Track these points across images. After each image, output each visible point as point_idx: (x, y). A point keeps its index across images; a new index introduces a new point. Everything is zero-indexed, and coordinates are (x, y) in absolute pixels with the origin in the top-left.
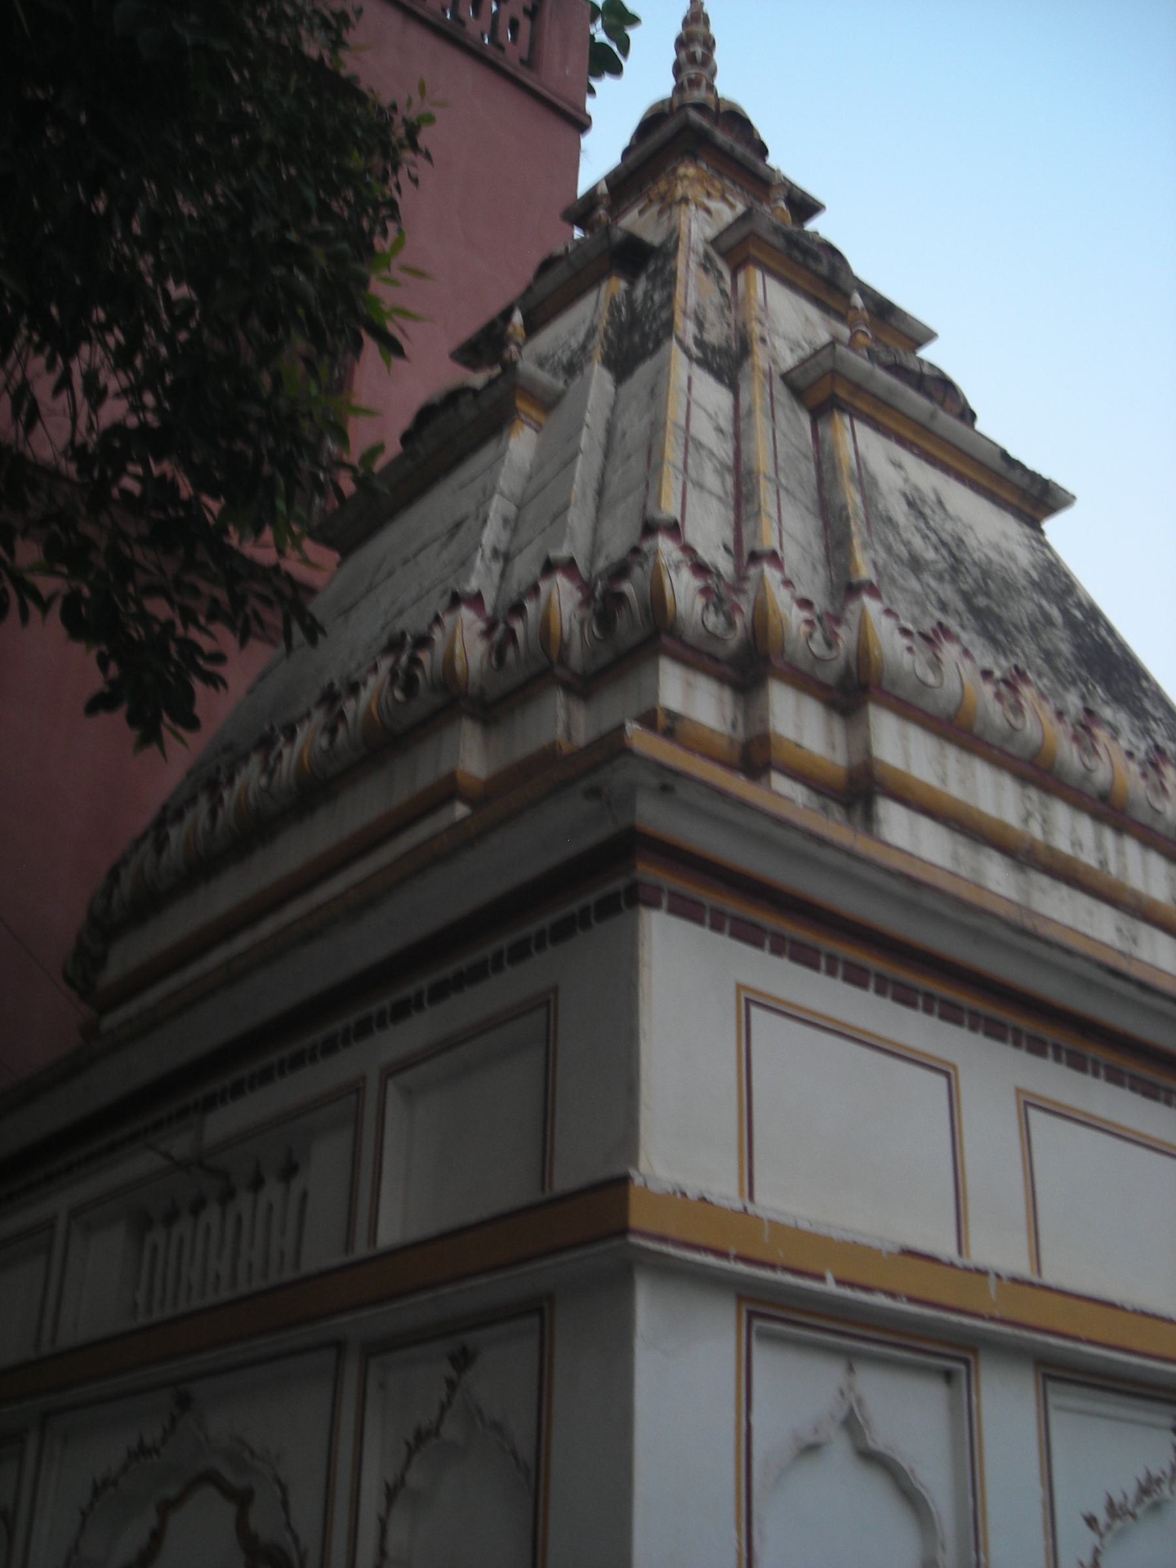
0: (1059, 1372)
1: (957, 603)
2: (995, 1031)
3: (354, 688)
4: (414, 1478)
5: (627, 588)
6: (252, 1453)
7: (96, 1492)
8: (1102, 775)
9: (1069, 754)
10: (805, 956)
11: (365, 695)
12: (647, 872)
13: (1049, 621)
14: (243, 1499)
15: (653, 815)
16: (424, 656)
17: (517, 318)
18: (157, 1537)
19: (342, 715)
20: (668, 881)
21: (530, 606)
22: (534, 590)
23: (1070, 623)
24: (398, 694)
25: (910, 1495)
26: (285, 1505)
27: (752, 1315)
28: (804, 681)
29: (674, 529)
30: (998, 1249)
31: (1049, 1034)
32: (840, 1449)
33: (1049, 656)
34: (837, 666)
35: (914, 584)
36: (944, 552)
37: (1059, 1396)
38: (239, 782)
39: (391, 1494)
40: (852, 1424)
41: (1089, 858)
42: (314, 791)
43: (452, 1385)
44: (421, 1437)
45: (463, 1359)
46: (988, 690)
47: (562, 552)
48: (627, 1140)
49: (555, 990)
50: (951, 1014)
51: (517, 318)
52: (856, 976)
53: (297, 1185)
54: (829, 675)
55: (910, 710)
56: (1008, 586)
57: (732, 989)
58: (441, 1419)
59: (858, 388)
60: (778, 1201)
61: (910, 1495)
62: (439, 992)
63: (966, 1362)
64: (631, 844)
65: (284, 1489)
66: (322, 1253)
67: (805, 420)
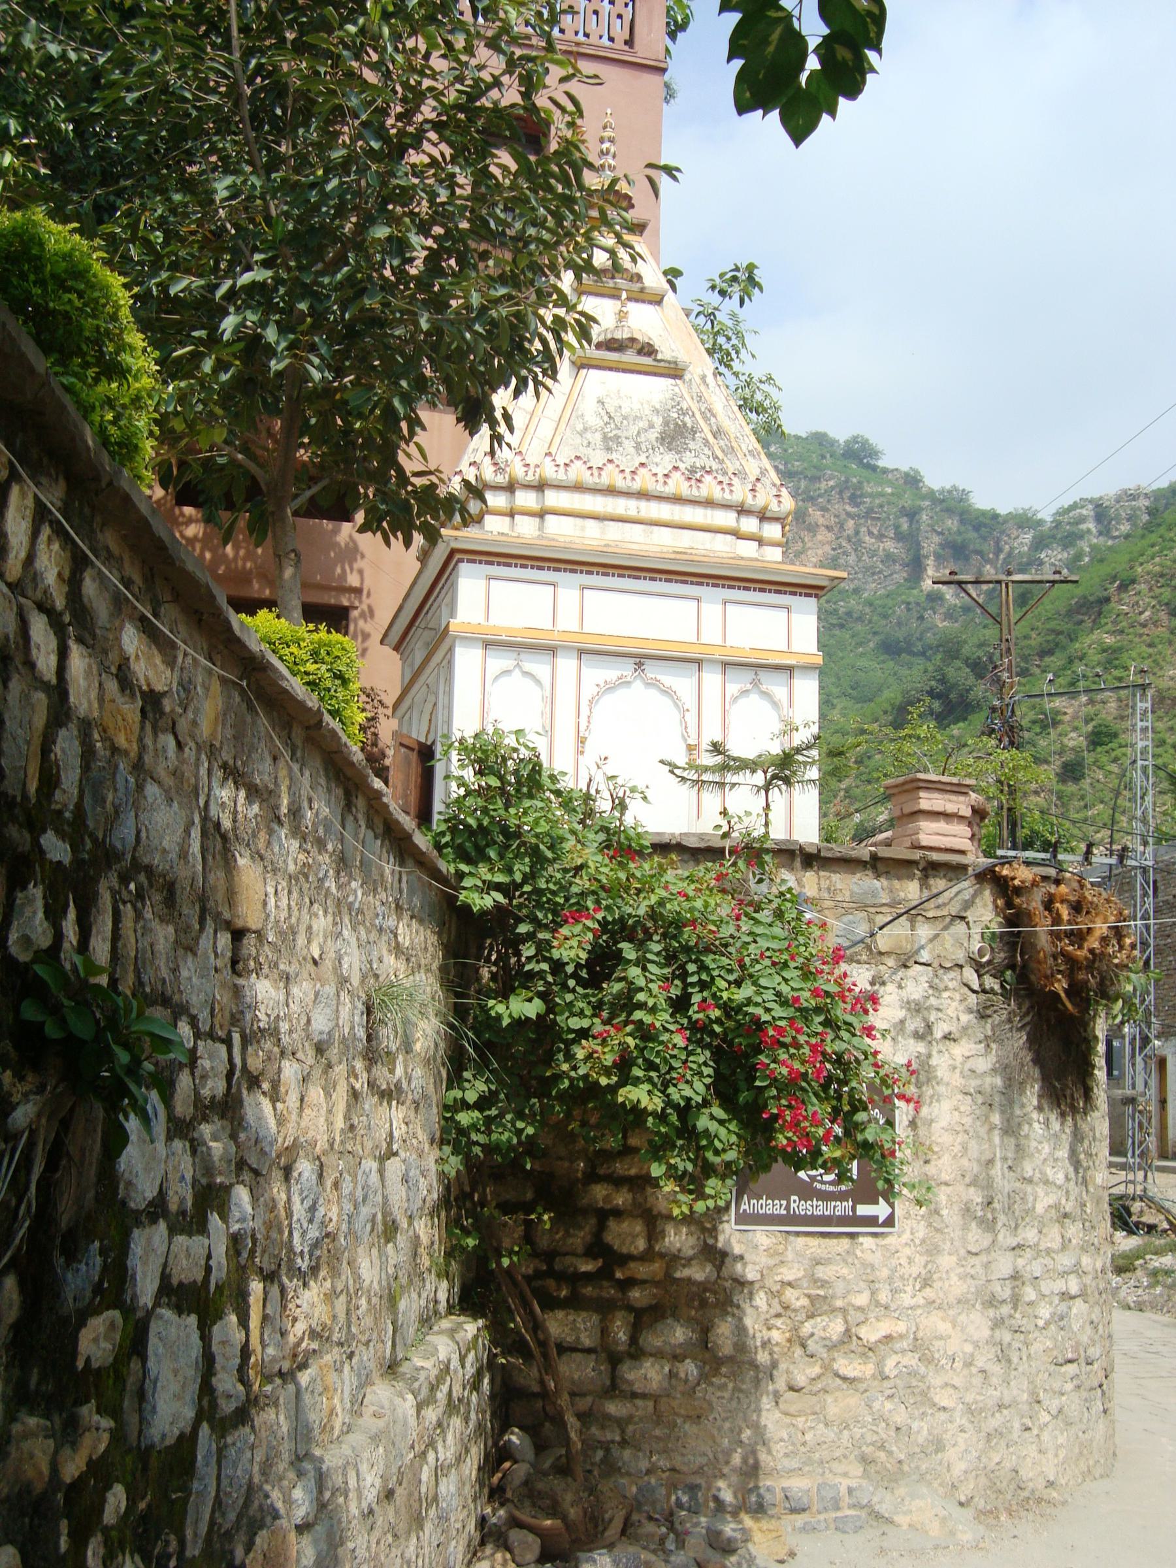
0: (582, 652)
2: (572, 571)
8: (636, 486)
9: (620, 483)
10: (509, 565)
13: (651, 426)
20: (466, 557)
23: (666, 423)
25: (538, 682)
28: (528, 487)
31: (595, 569)
32: (517, 672)
33: (638, 447)
35: (578, 440)
36: (606, 419)
41: (632, 513)
50: (555, 570)
52: (524, 566)
55: (559, 487)
56: (637, 418)
60: (491, 623)
61: (538, 682)
64: (453, 552)
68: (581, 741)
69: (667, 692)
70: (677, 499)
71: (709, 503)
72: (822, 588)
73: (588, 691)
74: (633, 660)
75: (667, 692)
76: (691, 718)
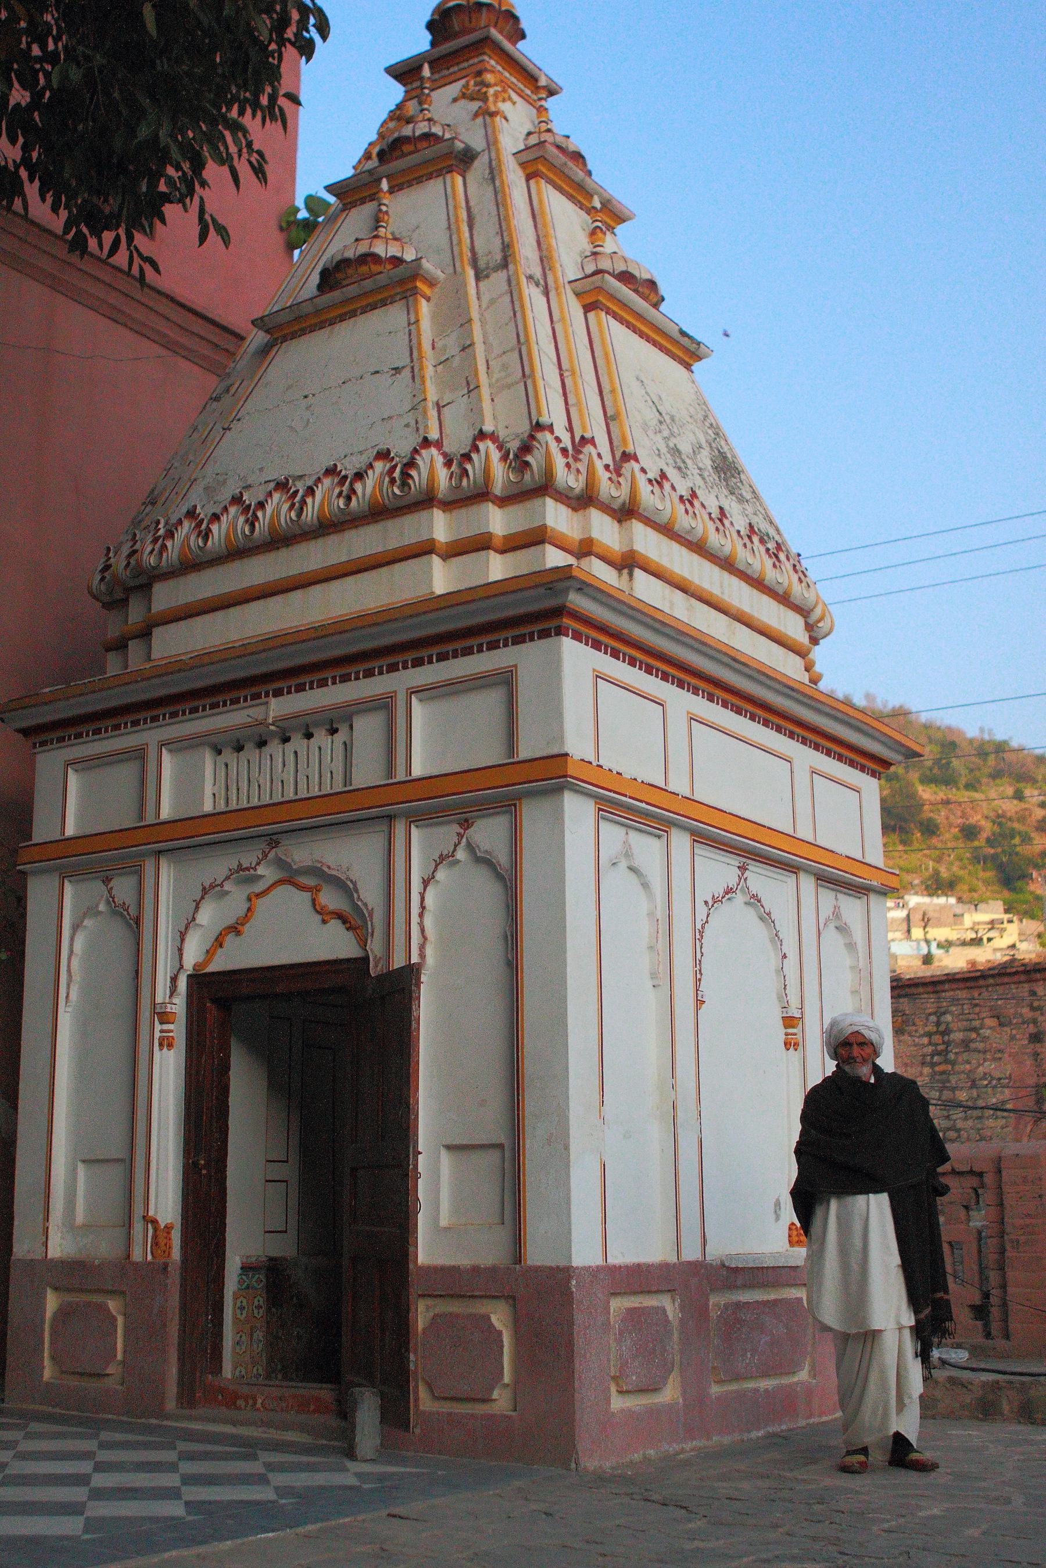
0: (699, 838)
1: (664, 450)
3: (359, 476)
4: (440, 875)
5: (529, 458)
6: (329, 867)
7: (205, 891)
8: (727, 550)
11: (370, 481)
12: (567, 621)
14: (315, 890)
15: (576, 600)
16: (414, 473)
17: (385, 185)
18: (249, 909)
19: (353, 491)
21: (474, 456)
22: (476, 449)
24: (397, 491)
25: (645, 886)
26: (357, 891)
27: (600, 810)
28: (606, 509)
29: (550, 428)
30: (679, 785)
34: (620, 501)
37: (700, 850)
38: (269, 508)
39: (426, 883)
40: (628, 854)
41: (716, 591)
42: (328, 527)
43: (460, 836)
44: (442, 858)
45: (466, 824)
46: (681, 508)
47: (488, 428)
48: (561, 738)
49: (516, 666)
51: (385, 185)
53: (340, 737)
54: (616, 505)
55: (648, 522)
57: (591, 673)
58: (455, 850)
59: (612, 297)
61: (645, 886)
62: (442, 657)
63: (667, 832)
65: (355, 884)
66: (367, 773)
67: (580, 312)
68: (699, 1002)
69: (766, 918)
70: (758, 584)
71: (784, 599)
72: (886, 764)
73: (701, 915)
74: (735, 861)
75: (766, 918)
76: (791, 966)
